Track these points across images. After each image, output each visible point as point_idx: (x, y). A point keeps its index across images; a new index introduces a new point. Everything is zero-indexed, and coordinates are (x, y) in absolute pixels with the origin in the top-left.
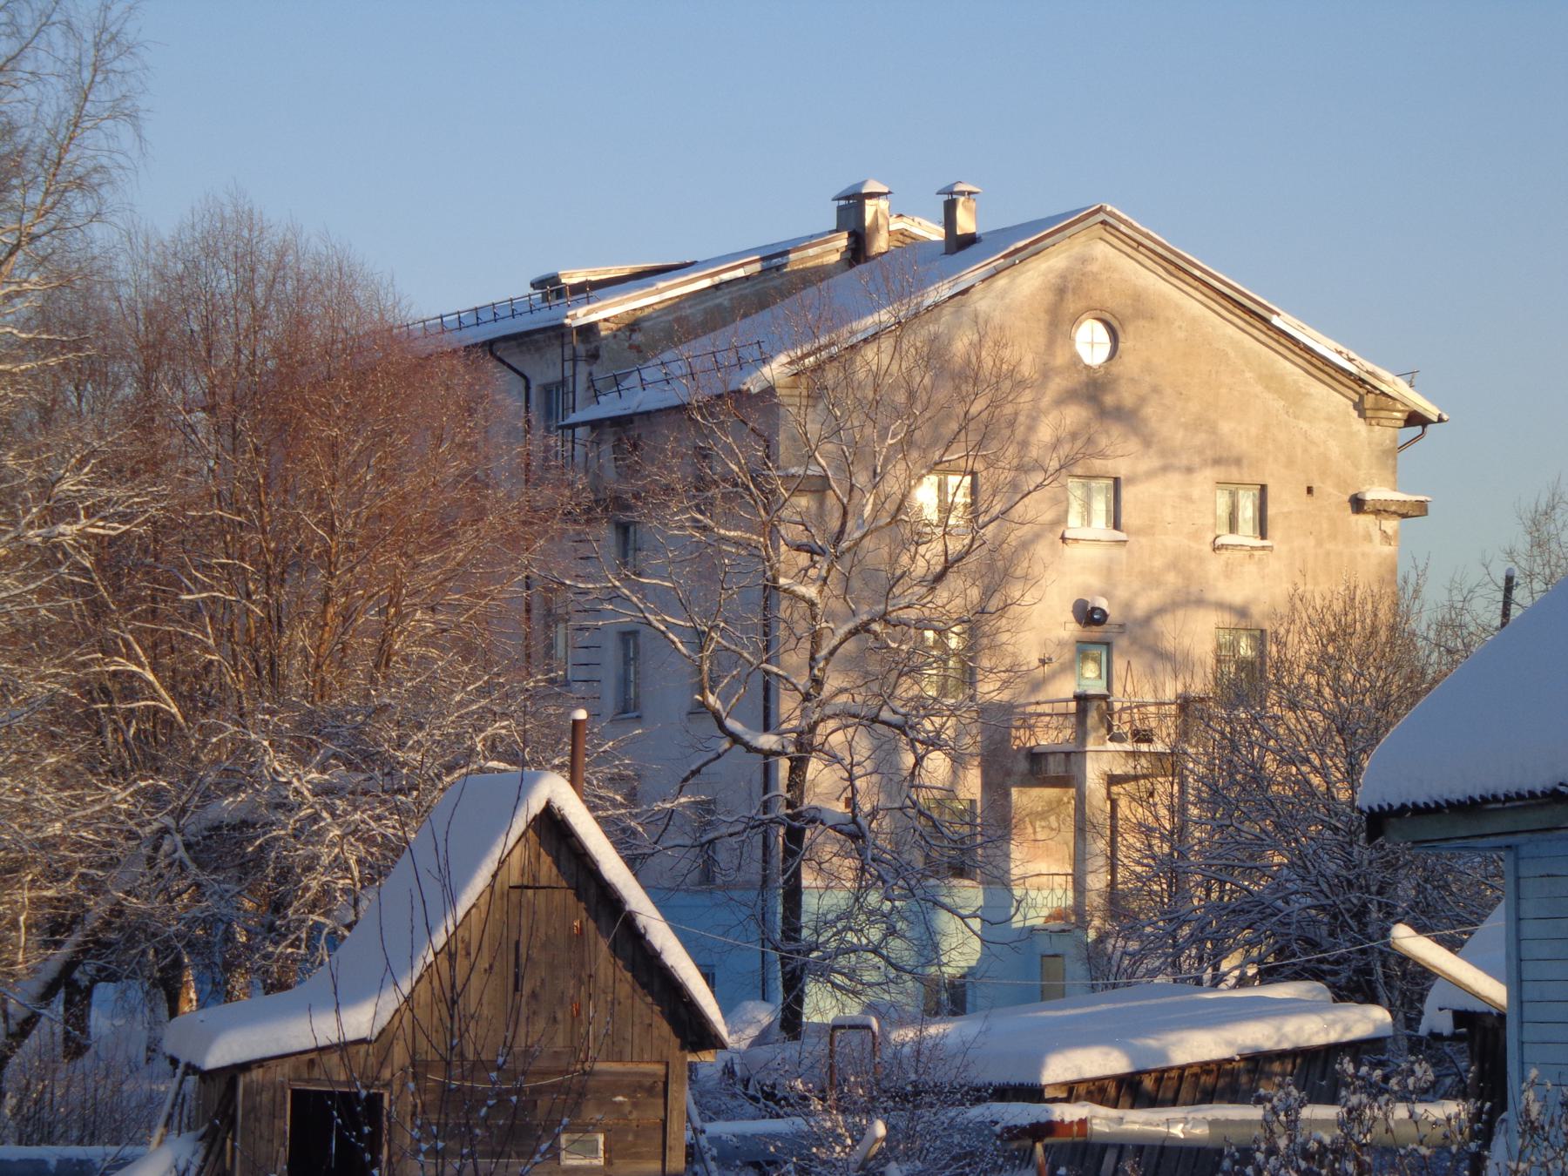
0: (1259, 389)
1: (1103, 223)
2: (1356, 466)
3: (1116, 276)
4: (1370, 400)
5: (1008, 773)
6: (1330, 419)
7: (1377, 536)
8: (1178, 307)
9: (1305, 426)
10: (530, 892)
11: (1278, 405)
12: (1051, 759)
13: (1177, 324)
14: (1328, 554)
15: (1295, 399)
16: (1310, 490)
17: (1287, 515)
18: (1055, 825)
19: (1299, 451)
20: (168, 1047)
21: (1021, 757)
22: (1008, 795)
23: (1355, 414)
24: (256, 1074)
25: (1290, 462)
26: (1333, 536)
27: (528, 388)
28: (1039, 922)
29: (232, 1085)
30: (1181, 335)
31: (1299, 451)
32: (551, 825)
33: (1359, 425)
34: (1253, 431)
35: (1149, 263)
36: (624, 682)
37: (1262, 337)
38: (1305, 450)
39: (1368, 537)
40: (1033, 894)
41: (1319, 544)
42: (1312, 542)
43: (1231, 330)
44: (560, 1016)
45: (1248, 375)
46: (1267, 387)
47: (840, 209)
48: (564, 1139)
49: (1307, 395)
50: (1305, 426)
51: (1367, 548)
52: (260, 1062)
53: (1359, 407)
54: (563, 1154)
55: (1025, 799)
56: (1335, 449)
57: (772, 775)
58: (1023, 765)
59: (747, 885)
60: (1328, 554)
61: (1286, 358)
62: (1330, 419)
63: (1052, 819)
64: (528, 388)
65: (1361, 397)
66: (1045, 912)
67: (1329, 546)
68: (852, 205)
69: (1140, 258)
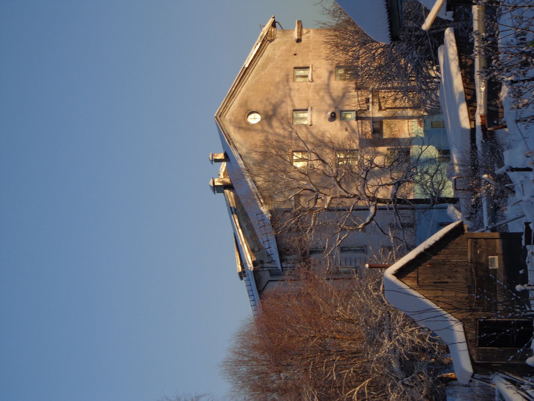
0: (266, 70)
1: (220, 116)
2: (288, 41)
4: (269, 38)
5: (379, 139)
6: (274, 50)
7: (308, 35)
8: (243, 94)
10: (419, 279)
11: (271, 65)
12: (375, 127)
14: (313, 49)
15: (269, 60)
16: (295, 55)
17: (302, 61)
20: (466, 383)
21: (374, 135)
22: (385, 139)
23: (273, 42)
24: (474, 357)
25: (287, 60)
26: (308, 47)
27: (271, 281)
28: (422, 129)
29: (477, 364)
30: (251, 93)
32: (400, 274)
33: (276, 41)
34: (278, 71)
35: (231, 103)
36: (355, 251)
38: (284, 56)
39: (308, 37)
40: (414, 131)
41: (310, 51)
42: (310, 54)
44: (455, 270)
46: (266, 68)
47: (218, 192)
48: (490, 268)
49: (268, 56)
51: (311, 38)
52: (471, 356)
53: (271, 41)
54: (495, 268)
56: (283, 48)
58: (377, 135)
62: (274, 50)
64: (271, 281)
65: (268, 40)
66: (419, 127)
67: (311, 48)
68: (217, 189)
69: (229, 106)
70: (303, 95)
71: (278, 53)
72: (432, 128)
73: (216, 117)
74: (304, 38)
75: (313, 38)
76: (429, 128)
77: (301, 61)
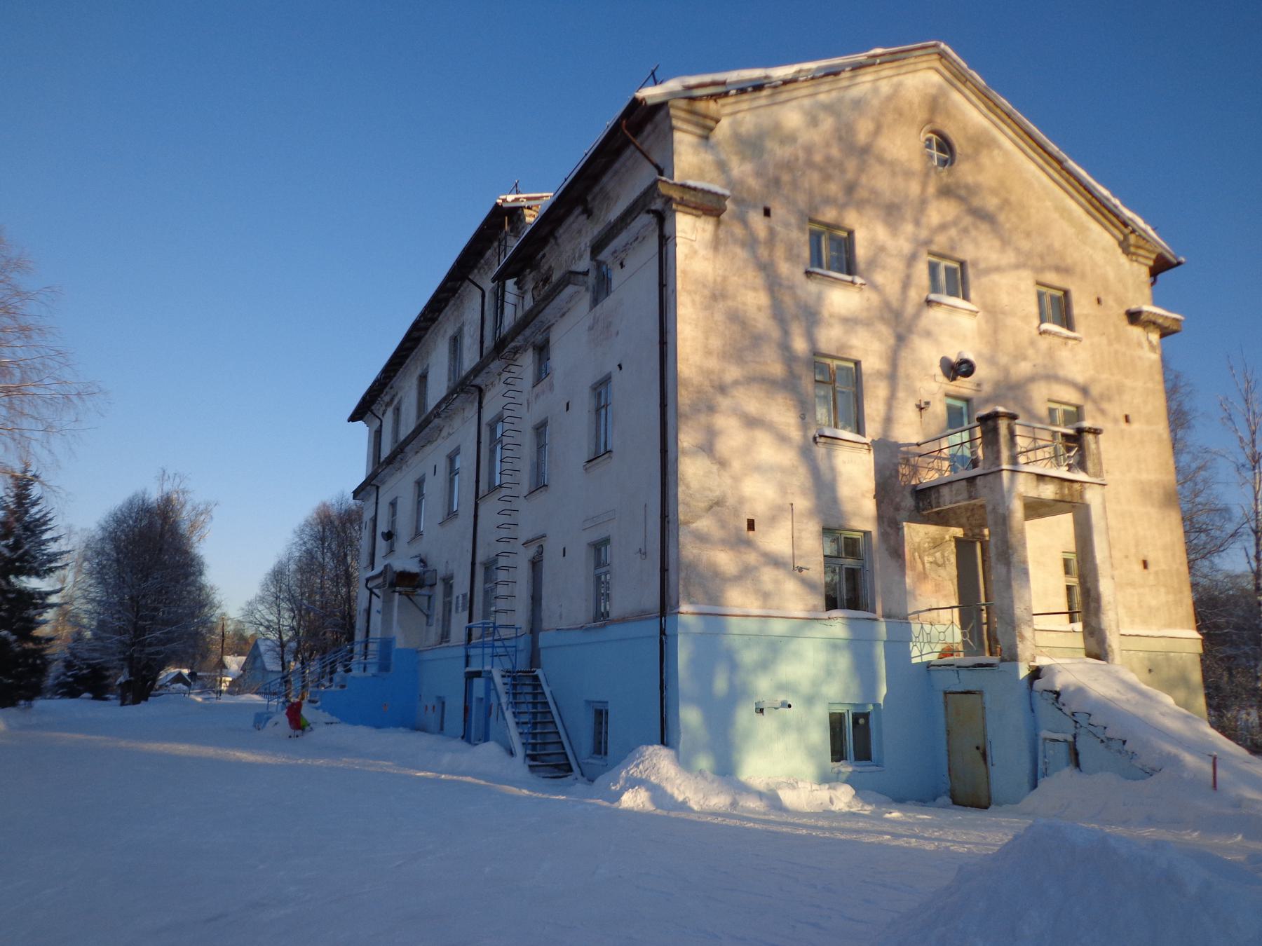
0: (1056, 216)
4: (1132, 238)
5: (897, 509)
6: (1104, 249)
7: (1146, 345)
11: (1070, 231)
12: (945, 491)
14: (1116, 352)
15: (1082, 230)
16: (1099, 301)
17: (1086, 316)
18: (940, 561)
21: (907, 493)
22: (899, 529)
23: (1119, 251)
28: (933, 658)
33: (1123, 259)
35: (974, 98)
37: (1056, 176)
39: (1140, 345)
40: (927, 628)
41: (1110, 344)
42: (1104, 341)
43: (1033, 167)
55: (917, 534)
56: (1111, 274)
57: (671, 493)
58: (909, 502)
59: (642, 616)
60: (1116, 352)
61: (1072, 197)
62: (1104, 249)
63: (938, 555)
65: (1126, 237)
66: (939, 648)
67: (1116, 346)
71: (1099, 257)
72: (946, 693)
74: (1136, 331)
75: (1140, 358)
76: (952, 682)
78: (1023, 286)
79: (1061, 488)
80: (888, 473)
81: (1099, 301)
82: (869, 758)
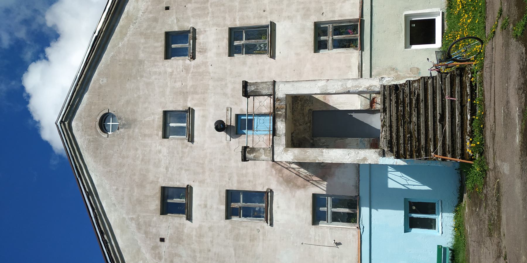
0: (126, 39)
3: (83, 114)
9: (141, 13)
13: (101, 83)
16: (167, 8)
17: (178, 20)
19: (151, 15)
25: (156, 20)
30: (105, 80)
31: (151, 15)
34: (143, 41)
38: (150, 12)
42: (189, 6)
45: (120, 45)
46: (126, 34)
50: (141, 13)
70: (178, 85)
73: (56, 124)
77: (175, 21)
78: (169, 70)
79: (280, 116)
80: (281, 179)
81: (167, 8)
82: (434, 204)
